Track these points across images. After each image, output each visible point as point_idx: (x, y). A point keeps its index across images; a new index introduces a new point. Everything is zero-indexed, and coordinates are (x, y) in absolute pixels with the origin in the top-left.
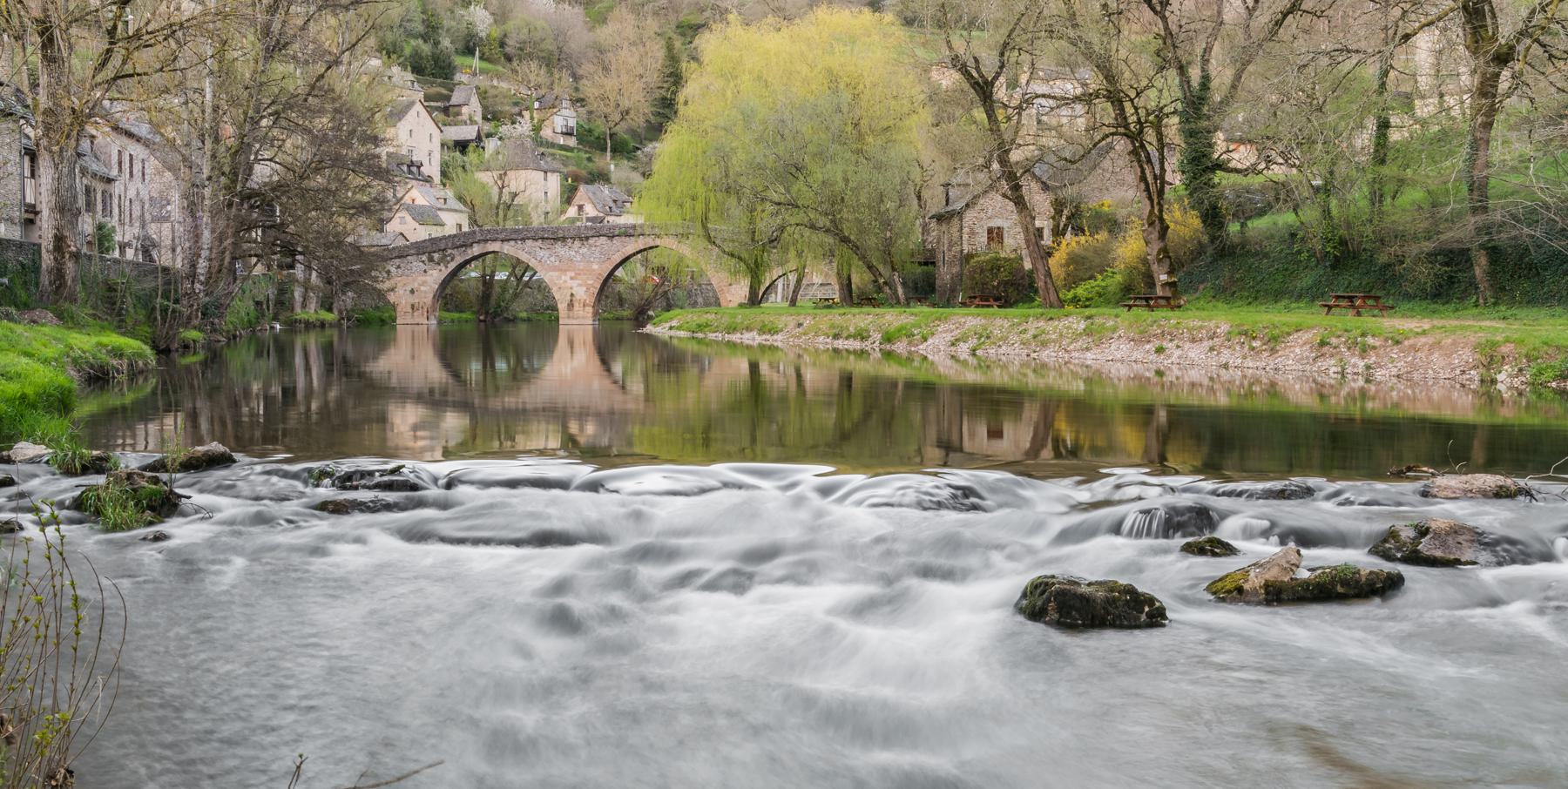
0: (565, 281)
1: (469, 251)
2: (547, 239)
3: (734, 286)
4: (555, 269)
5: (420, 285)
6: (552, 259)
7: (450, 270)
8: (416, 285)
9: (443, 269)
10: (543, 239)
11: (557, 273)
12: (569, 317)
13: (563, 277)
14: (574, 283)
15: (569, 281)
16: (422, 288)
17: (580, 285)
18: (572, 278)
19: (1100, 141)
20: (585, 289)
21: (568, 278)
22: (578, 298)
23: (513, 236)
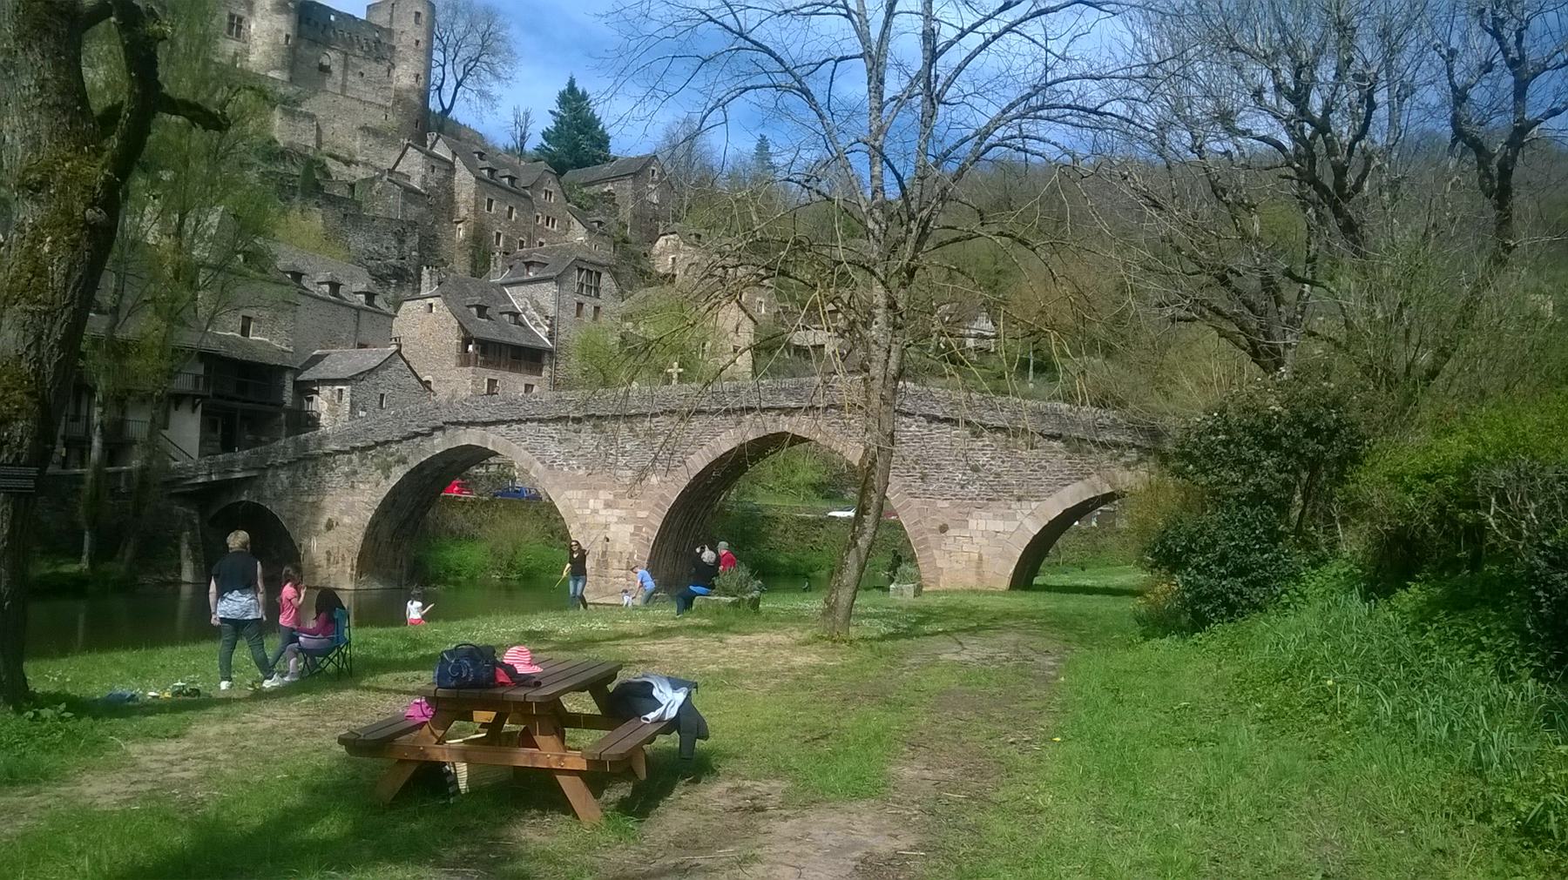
0: (595, 511)
1: (427, 444)
2: (566, 418)
3: (951, 532)
4: (576, 484)
5: (342, 512)
6: (573, 462)
7: (393, 481)
8: (336, 514)
9: (383, 482)
10: (559, 419)
11: (580, 494)
12: (598, 590)
13: (591, 501)
14: (612, 515)
15: (603, 512)
16: (346, 520)
17: (622, 520)
18: (608, 505)
19: (1061, 81)
20: (631, 528)
21: (600, 505)
22: (618, 548)
23: (507, 416)
